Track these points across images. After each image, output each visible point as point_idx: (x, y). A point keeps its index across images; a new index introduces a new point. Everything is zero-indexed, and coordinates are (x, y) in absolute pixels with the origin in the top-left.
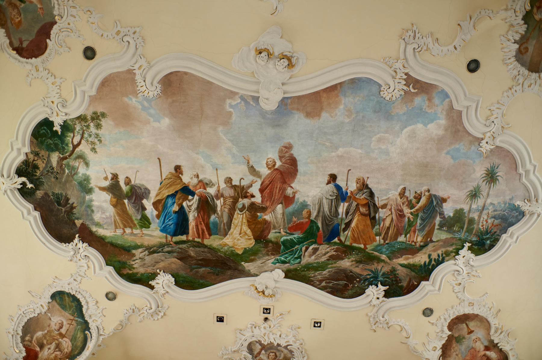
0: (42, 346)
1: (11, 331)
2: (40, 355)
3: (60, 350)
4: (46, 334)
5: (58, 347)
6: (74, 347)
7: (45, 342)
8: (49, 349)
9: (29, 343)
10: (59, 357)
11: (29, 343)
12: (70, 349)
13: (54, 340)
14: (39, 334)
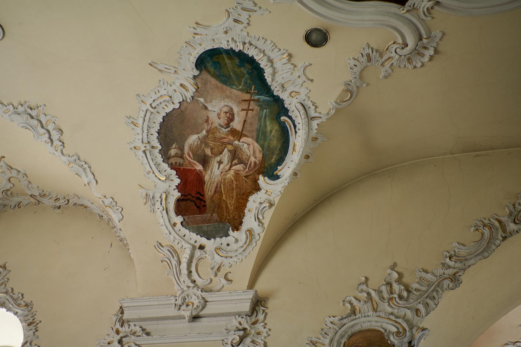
0: (205, 161)
2: (207, 178)
3: (241, 162)
5: (236, 155)
6: (267, 151)
7: (208, 152)
8: (220, 163)
10: (243, 173)
12: (259, 156)
13: (224, 145)
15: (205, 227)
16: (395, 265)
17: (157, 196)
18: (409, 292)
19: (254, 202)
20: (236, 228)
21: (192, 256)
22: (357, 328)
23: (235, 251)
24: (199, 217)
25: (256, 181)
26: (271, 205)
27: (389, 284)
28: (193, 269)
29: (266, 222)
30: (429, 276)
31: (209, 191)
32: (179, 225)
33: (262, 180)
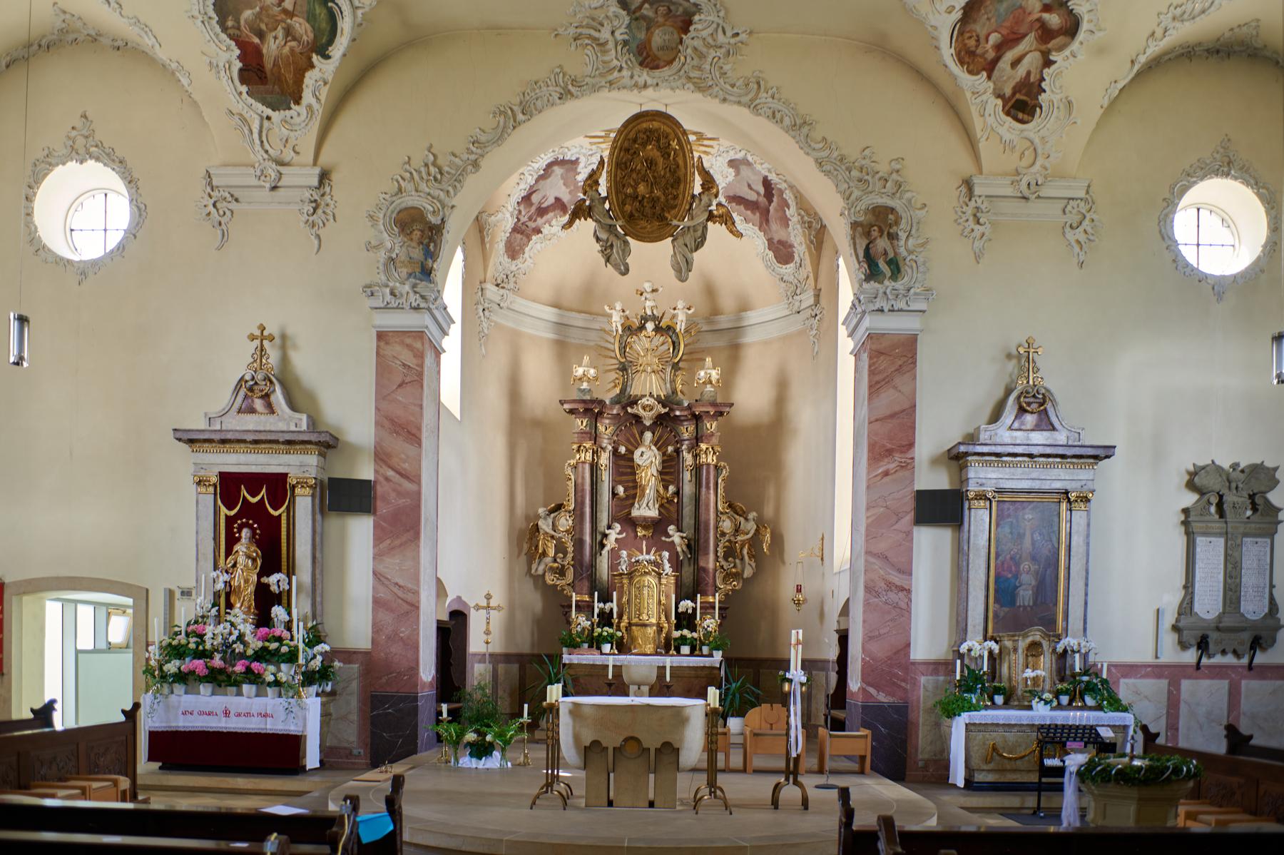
0: (261, 35)
1: (196, 13)
2: (264, 51)
3: (294, 39)
4: (260, 13)
5: (289, 32)
6: (317, 32)
7: (263, 27)
8: (275, 38)
9: (237, 32)
10: (298, 50)
11: (237, 32)
12: (311, 36)
13: (278, 22)
14: (247, 14)
15: (269, 98)
16: (431, 146)
17: (221, 65)
18: (441, 174)
19: (310, 78)
20: (298, 102)
21: (261, 127)
22: (403, 205)
23: (297, 125)
24: (262, 87)
25: (310, 58)
26: (325, 83)
27: (426, 165)
28: (264, 139)
29: (323, 98)
30: (457, 160)
31: (268, 64)
32: (245, 95)
33: (315, 58)
